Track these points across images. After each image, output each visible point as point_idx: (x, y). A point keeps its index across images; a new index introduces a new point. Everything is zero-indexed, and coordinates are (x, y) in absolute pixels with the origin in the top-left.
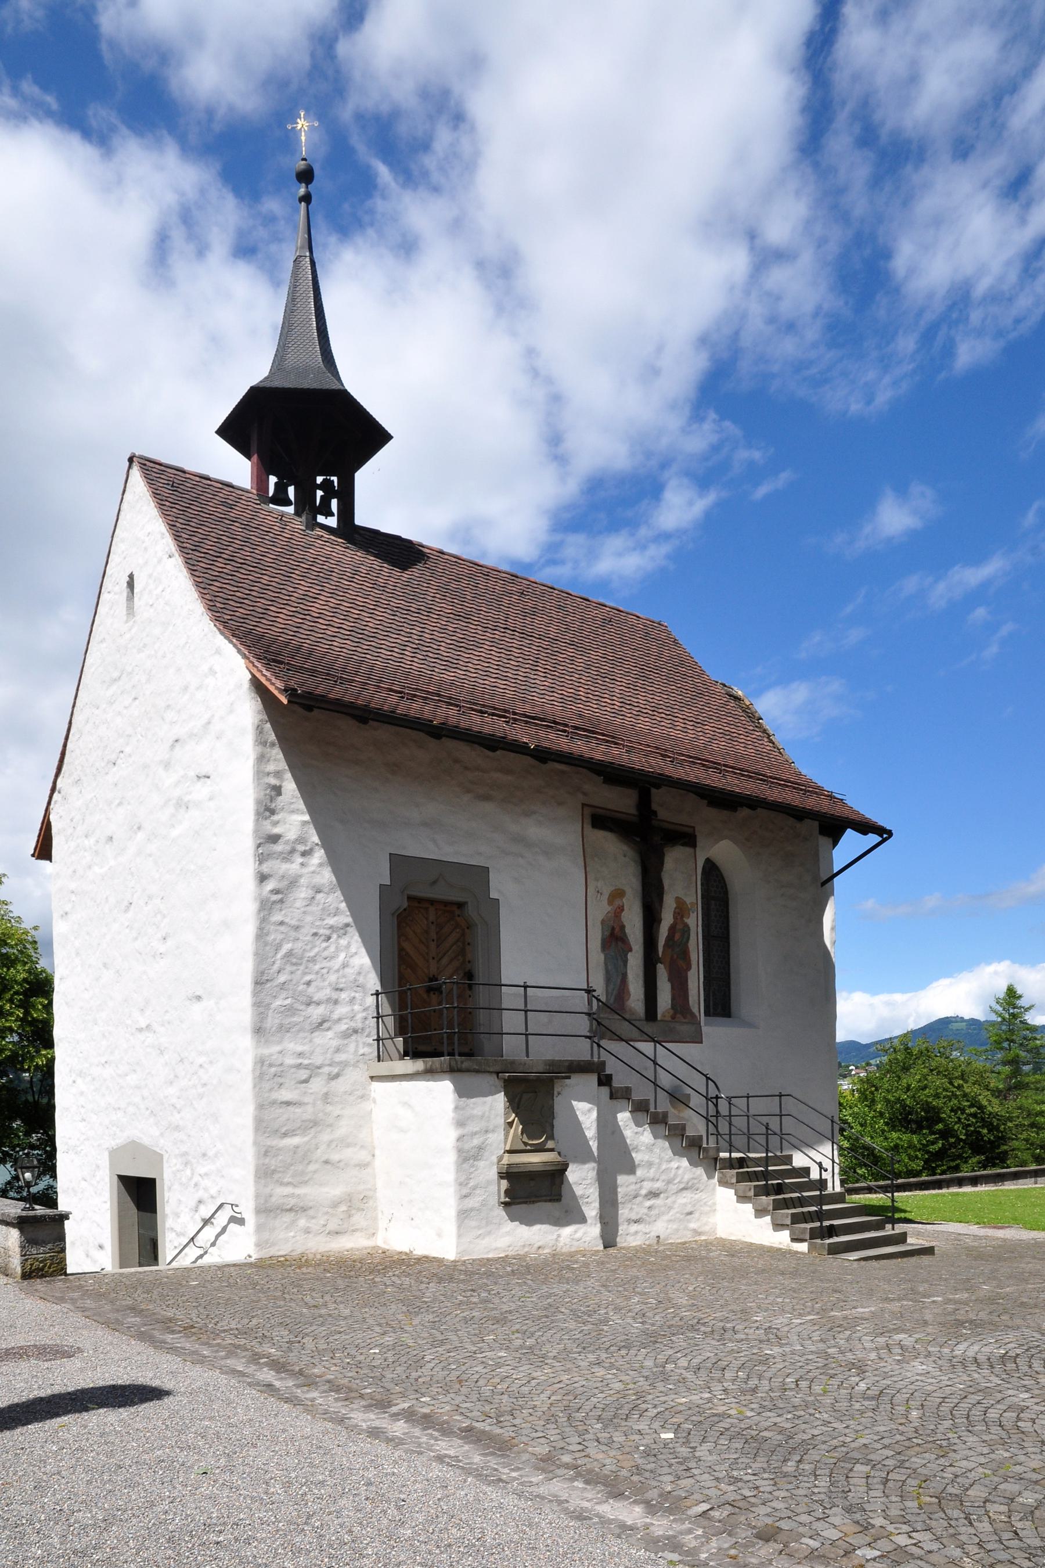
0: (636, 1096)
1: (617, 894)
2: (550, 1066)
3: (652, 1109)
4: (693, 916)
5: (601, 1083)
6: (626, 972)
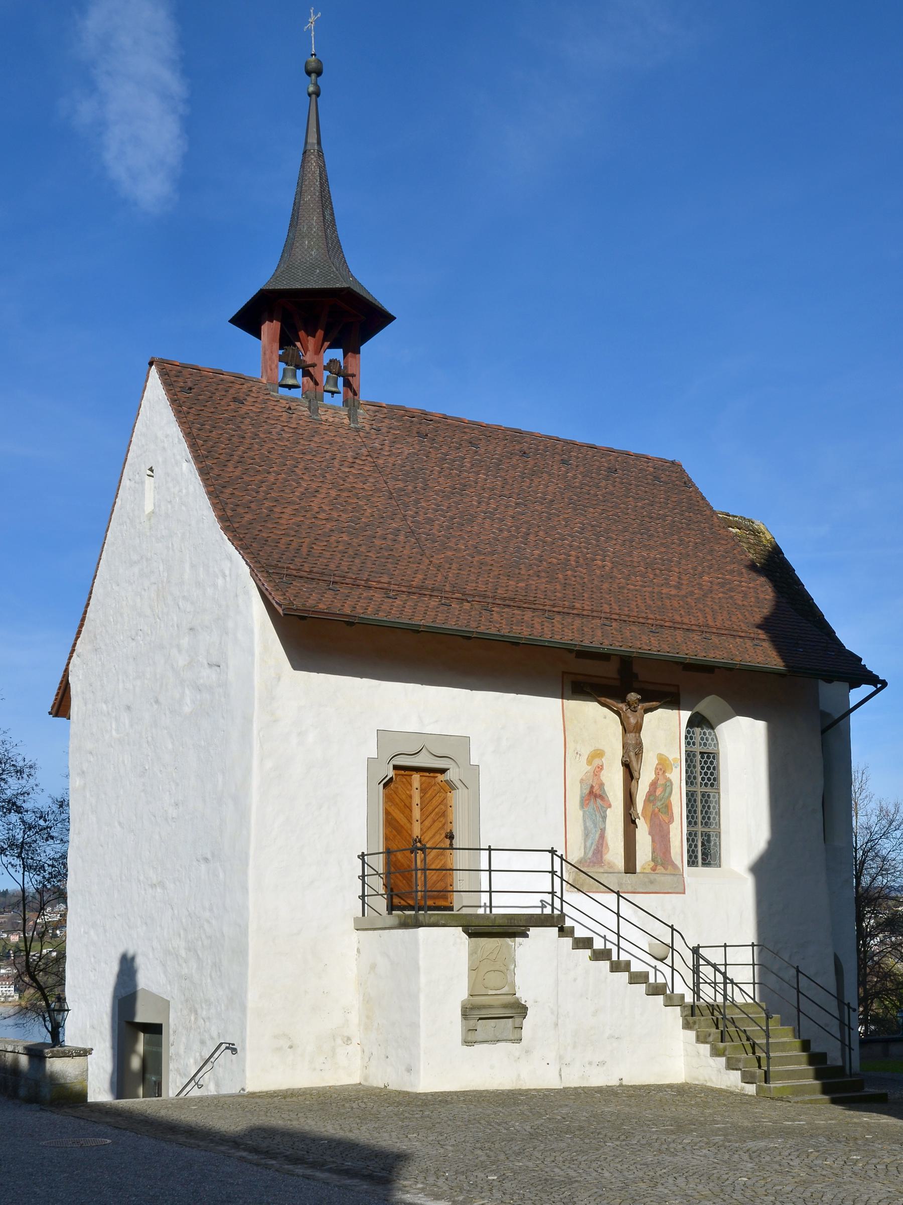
1: (598, 754)
2: (508, 919)
4: (676, 771)
6: (605, 828)
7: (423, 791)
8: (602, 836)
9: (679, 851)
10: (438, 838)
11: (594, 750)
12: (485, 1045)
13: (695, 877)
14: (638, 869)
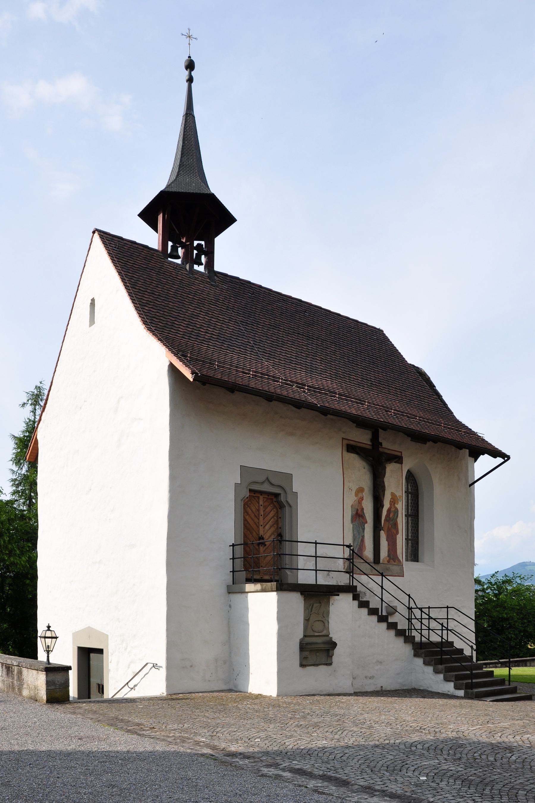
0: (371, 606)
1: (360, 490)
3: (380, 614)
4: (400, 503)
5: (354, 599)
6: (364, 535)
11: (359, 488)
12: (313, 667)
13: (408, 567)
14: (381, 562)
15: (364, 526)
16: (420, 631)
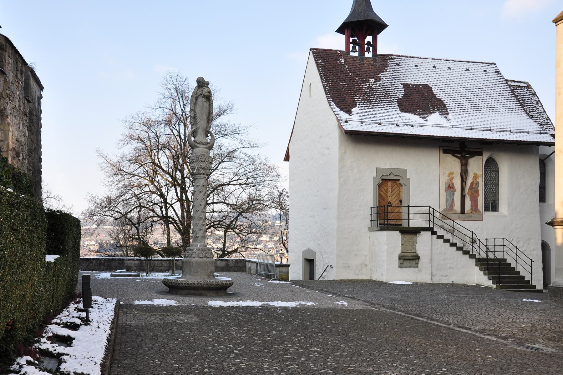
1: (452, 173)
7: (392, 187)
8: (453, 201)
9: (481, 206)
10: (397, 202)
14: (466, 213)
15: (454, 193)
16: (494, 253)
